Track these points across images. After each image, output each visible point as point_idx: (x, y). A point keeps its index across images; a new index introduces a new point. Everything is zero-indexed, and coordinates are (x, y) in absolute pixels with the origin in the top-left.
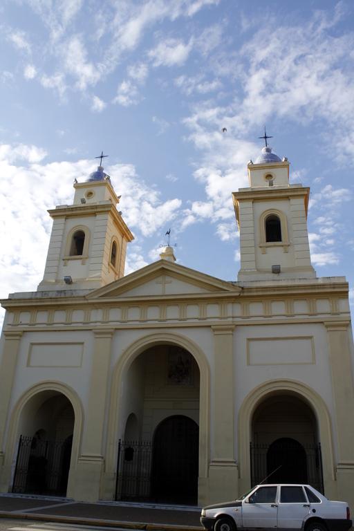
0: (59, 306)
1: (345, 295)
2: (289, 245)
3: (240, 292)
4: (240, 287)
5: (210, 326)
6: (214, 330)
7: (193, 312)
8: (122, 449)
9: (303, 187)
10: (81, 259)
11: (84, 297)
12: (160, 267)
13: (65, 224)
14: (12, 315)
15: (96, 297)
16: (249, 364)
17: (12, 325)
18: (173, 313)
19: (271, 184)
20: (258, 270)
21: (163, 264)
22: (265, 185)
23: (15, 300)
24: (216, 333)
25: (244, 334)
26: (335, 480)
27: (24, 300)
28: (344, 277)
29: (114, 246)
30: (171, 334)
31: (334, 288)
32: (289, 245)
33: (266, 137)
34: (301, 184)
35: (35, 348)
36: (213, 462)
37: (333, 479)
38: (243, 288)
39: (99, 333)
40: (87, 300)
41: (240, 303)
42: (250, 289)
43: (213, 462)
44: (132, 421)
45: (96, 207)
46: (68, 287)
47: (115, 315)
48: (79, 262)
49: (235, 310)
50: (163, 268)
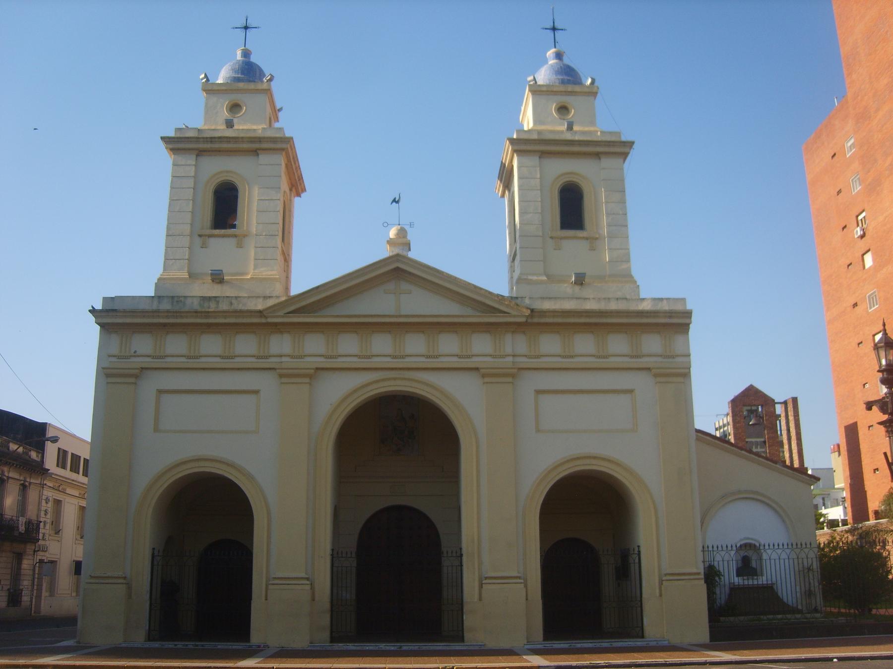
0: (209, 325)
1: (684, 328)
3: (527, 317)
4: (528, 308)
5: (477, 369)
6: (484, 376)
7: (448, 344)
9: (623, 139)
10: (236, 236)
11: (260, 312)
13: (196, 166)
14: (115, 340)
15: (281, 313)
16: (538, 430)
17: (119, 357)
19: (570, 127)
21: (398, 261)
22: (557, 127)
23: (125, 311)
24: (487, 380)
25: (531, 383)
26: (661, 595)
27: (133, 313)
28: (683, 300)
30: (409, 379)
31: (670, 317)
32: (597, 239)
33: (554, 29)
34: (618, 134)
35: (165, 398)
36: (486, 578)
37: (658, 594)
38: (532, 311)
39: (286, 375)
40: (266, 317)
41: (524, 333)
42: (543, 313)
43: (486, 578)
45: (260, 140)
46: (214, 291)
48: (233, 241)
50: (397, 269)
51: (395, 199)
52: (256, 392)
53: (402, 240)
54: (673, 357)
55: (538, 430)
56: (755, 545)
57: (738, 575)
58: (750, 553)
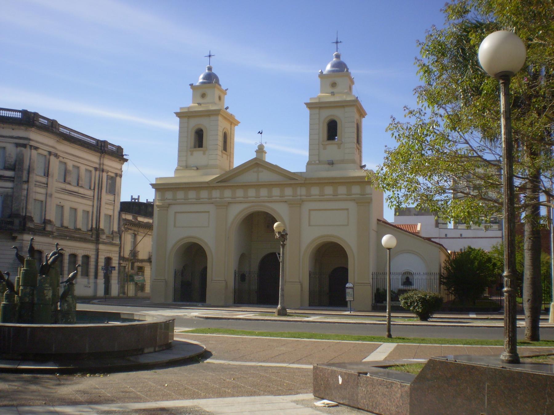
2: (341, 144)
7: (276, 192)
8: (237, 275)
11: (207, 182)
12: (255, 162)
18: (264, 192)
20: (319, 161)
29: (225, 136)
33: (337, 42)
44: (243, 258)
47: (228, 193)
49: (302, 191)
51: (260, 132)
52: (208, 212)
53: (261, 150)
54: (365, 195)
55: (309, 225)
56: (411, 273)
57: (401, 285)
58: (410, 277)
